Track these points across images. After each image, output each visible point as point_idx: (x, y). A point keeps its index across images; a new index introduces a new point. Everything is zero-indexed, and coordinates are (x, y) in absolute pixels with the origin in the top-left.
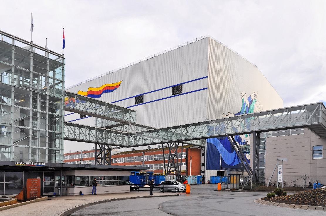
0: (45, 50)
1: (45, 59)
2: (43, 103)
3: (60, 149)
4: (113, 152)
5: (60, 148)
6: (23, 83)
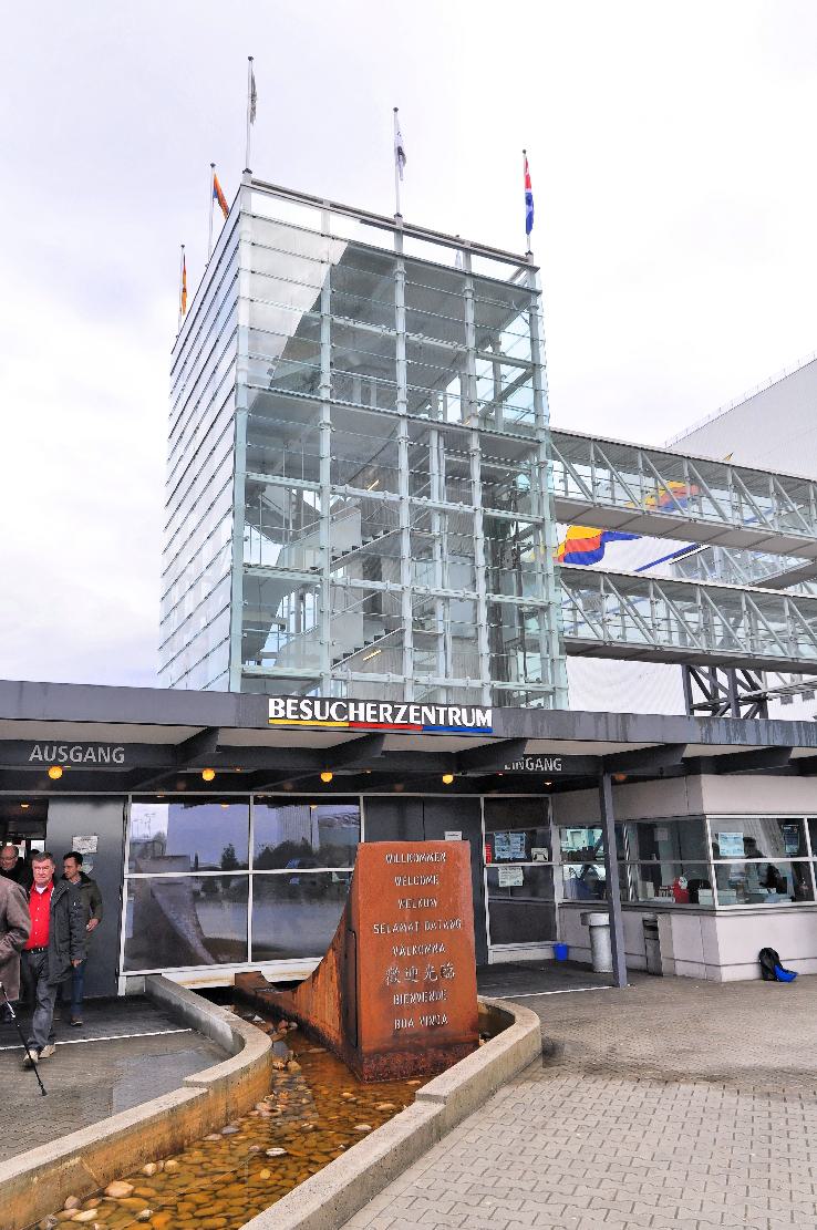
1: (451, 279)
2: (457, 476)
3: (548, 688)
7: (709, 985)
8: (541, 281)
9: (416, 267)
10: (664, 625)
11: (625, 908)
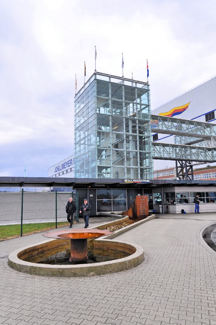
0: (132, 81)
1: (133, 89)
2: (134, 127)
4: (194, 168)
5: (149, 166)
6: (115, 113)
7: (174, 214)
8: (150, 88)
9: (126, 87)
10: (172, 153)
11: (164, 204)
